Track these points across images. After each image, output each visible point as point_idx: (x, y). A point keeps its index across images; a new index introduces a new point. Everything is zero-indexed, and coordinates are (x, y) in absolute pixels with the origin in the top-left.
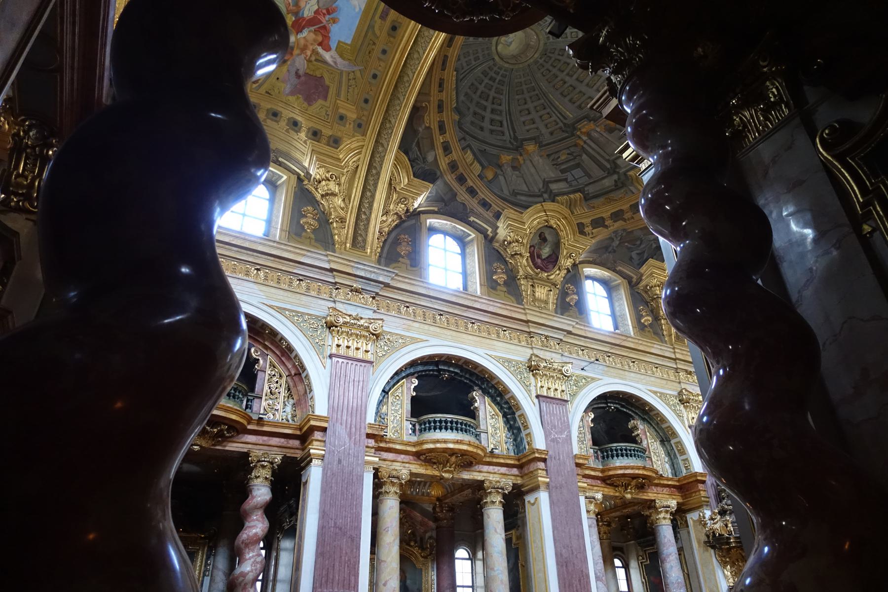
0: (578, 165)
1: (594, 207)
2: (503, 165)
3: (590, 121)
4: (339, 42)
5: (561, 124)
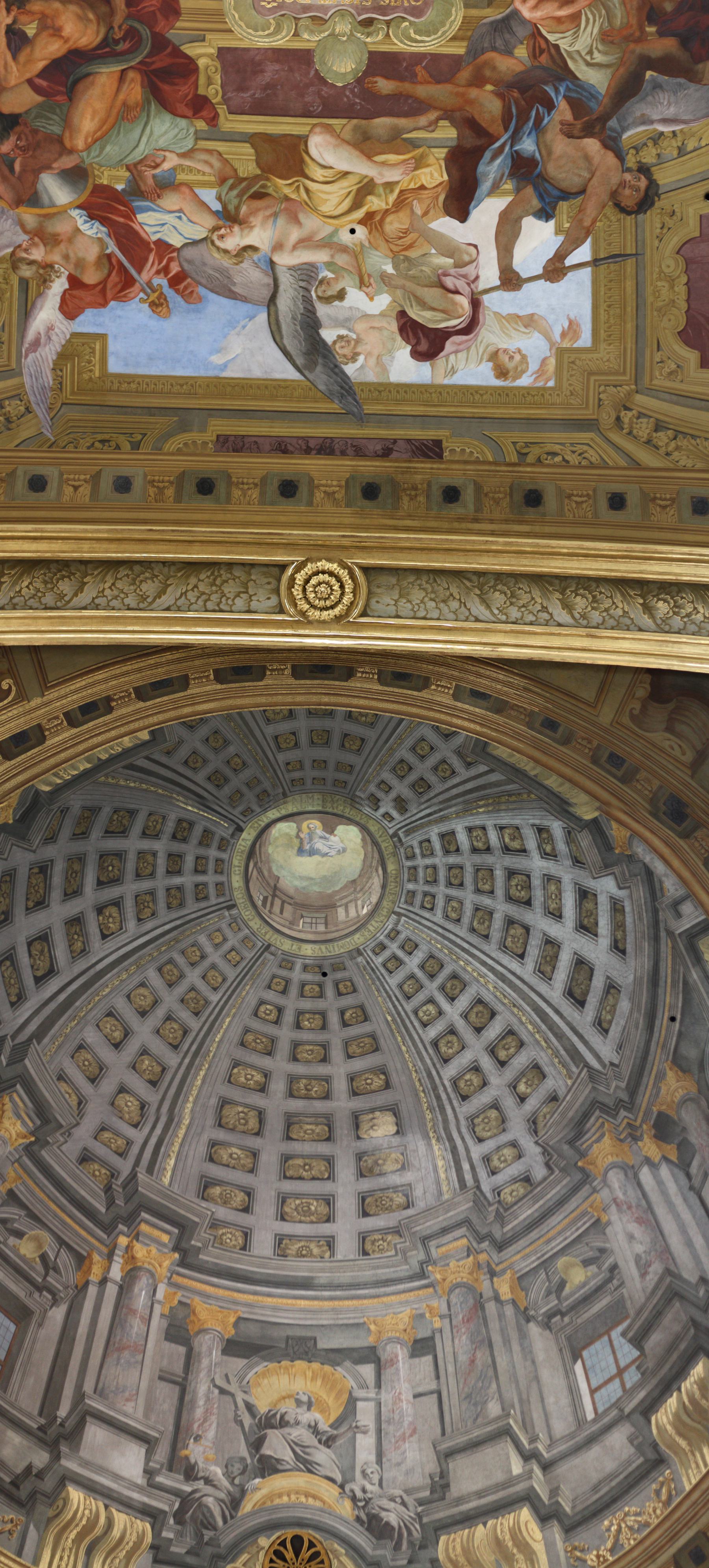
3: (176, 1249)
4: (102, 338)
5: (125, 1167)
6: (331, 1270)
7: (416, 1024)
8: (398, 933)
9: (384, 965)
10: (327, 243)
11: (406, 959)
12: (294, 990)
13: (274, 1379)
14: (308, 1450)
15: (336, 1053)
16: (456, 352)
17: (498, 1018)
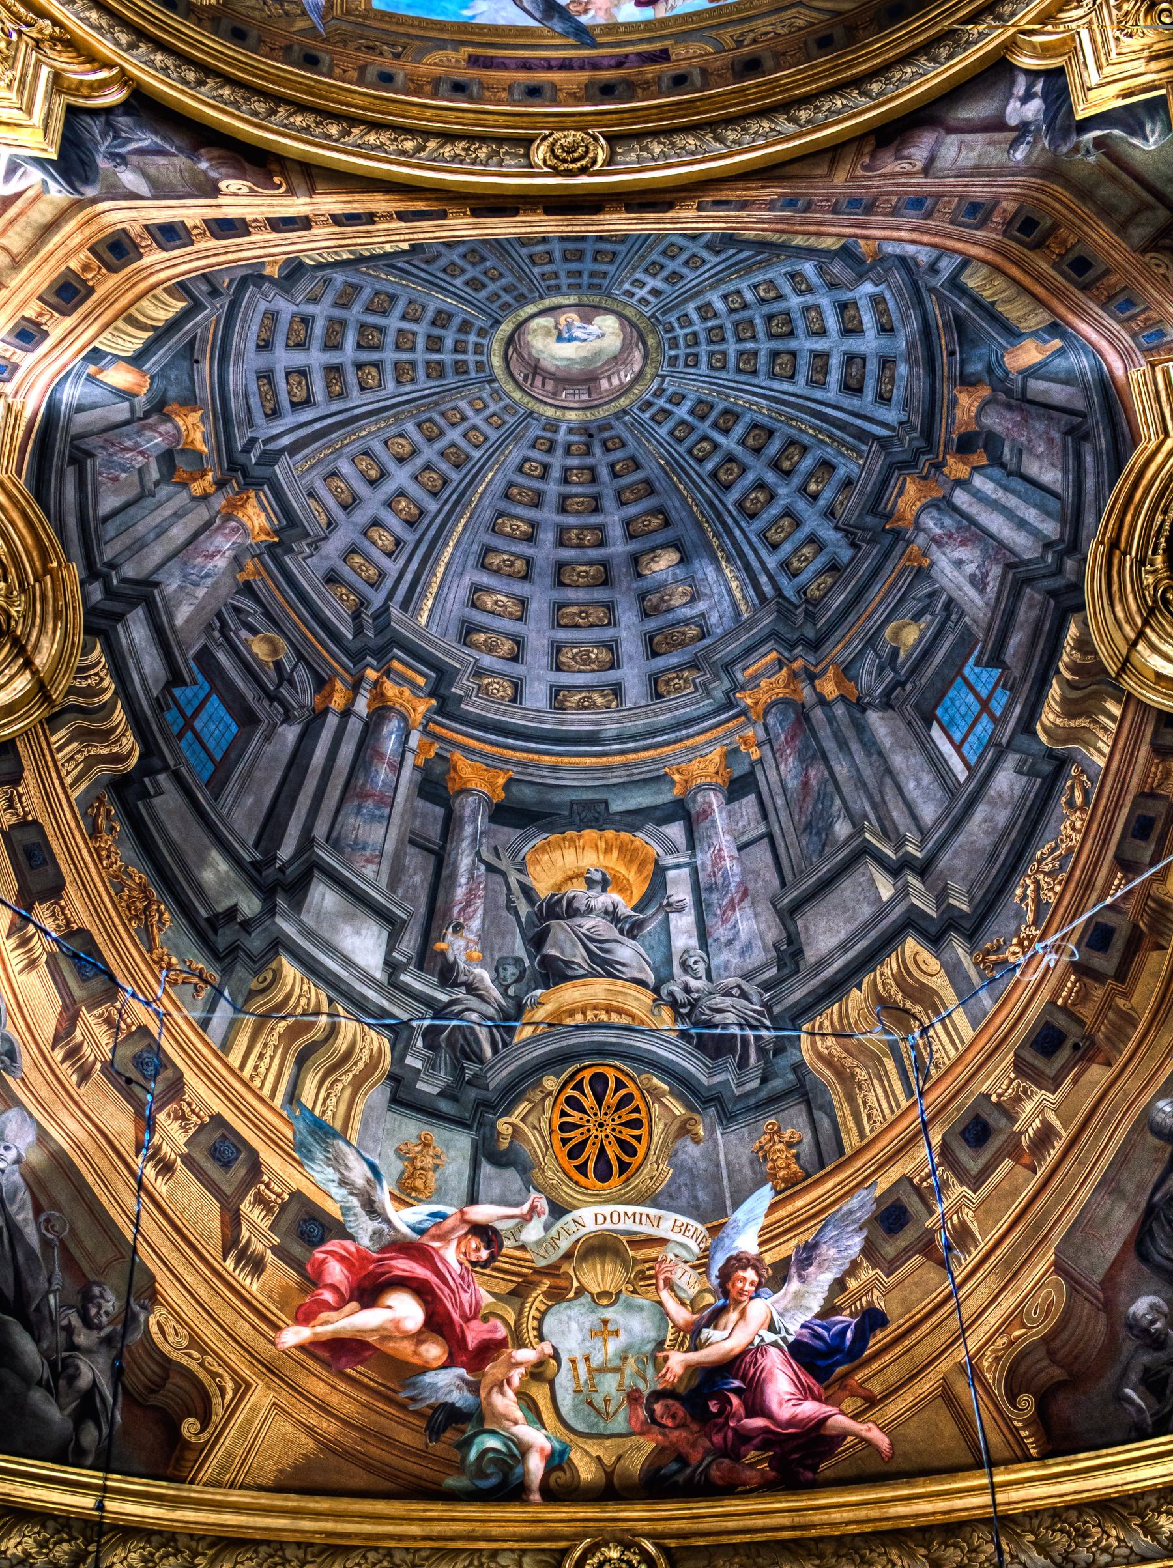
0: (247, 719)
1: (94, 832)
2: (168, 418)
3: (432, 694)
6: (619, 720)
7: (692, 462)
8: (664, 390)
9: (652, 418)
11: (675, 409)
12: (559, 452)
13: (557, 855)
14: (606, 946)
15: (609, 502)
17: (777, 434)
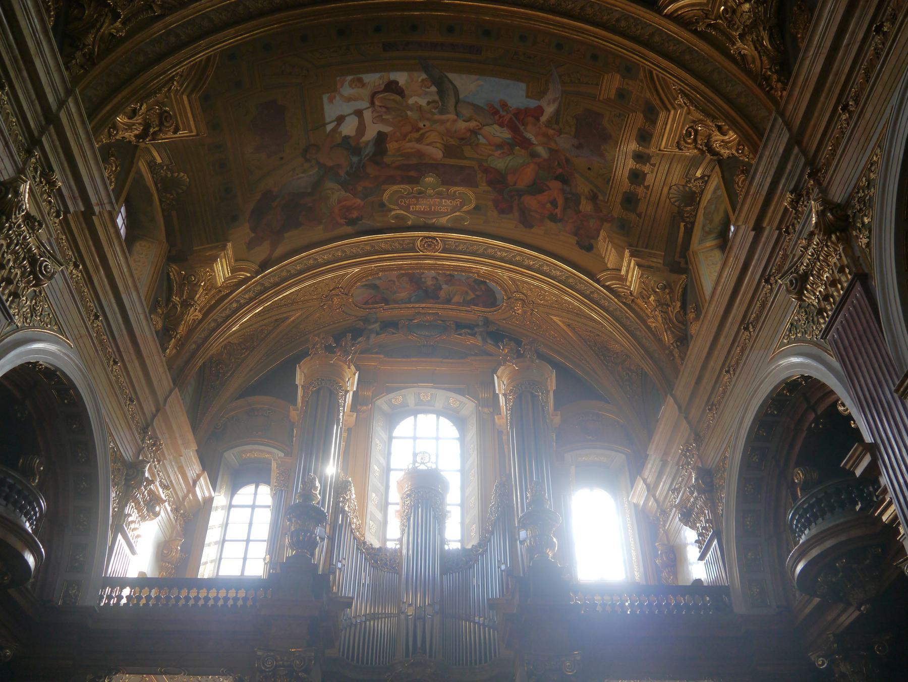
4: (527, 96)
10: (436, 122)
16: (380, 85)
